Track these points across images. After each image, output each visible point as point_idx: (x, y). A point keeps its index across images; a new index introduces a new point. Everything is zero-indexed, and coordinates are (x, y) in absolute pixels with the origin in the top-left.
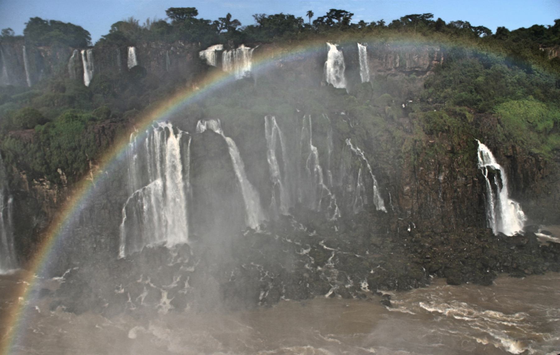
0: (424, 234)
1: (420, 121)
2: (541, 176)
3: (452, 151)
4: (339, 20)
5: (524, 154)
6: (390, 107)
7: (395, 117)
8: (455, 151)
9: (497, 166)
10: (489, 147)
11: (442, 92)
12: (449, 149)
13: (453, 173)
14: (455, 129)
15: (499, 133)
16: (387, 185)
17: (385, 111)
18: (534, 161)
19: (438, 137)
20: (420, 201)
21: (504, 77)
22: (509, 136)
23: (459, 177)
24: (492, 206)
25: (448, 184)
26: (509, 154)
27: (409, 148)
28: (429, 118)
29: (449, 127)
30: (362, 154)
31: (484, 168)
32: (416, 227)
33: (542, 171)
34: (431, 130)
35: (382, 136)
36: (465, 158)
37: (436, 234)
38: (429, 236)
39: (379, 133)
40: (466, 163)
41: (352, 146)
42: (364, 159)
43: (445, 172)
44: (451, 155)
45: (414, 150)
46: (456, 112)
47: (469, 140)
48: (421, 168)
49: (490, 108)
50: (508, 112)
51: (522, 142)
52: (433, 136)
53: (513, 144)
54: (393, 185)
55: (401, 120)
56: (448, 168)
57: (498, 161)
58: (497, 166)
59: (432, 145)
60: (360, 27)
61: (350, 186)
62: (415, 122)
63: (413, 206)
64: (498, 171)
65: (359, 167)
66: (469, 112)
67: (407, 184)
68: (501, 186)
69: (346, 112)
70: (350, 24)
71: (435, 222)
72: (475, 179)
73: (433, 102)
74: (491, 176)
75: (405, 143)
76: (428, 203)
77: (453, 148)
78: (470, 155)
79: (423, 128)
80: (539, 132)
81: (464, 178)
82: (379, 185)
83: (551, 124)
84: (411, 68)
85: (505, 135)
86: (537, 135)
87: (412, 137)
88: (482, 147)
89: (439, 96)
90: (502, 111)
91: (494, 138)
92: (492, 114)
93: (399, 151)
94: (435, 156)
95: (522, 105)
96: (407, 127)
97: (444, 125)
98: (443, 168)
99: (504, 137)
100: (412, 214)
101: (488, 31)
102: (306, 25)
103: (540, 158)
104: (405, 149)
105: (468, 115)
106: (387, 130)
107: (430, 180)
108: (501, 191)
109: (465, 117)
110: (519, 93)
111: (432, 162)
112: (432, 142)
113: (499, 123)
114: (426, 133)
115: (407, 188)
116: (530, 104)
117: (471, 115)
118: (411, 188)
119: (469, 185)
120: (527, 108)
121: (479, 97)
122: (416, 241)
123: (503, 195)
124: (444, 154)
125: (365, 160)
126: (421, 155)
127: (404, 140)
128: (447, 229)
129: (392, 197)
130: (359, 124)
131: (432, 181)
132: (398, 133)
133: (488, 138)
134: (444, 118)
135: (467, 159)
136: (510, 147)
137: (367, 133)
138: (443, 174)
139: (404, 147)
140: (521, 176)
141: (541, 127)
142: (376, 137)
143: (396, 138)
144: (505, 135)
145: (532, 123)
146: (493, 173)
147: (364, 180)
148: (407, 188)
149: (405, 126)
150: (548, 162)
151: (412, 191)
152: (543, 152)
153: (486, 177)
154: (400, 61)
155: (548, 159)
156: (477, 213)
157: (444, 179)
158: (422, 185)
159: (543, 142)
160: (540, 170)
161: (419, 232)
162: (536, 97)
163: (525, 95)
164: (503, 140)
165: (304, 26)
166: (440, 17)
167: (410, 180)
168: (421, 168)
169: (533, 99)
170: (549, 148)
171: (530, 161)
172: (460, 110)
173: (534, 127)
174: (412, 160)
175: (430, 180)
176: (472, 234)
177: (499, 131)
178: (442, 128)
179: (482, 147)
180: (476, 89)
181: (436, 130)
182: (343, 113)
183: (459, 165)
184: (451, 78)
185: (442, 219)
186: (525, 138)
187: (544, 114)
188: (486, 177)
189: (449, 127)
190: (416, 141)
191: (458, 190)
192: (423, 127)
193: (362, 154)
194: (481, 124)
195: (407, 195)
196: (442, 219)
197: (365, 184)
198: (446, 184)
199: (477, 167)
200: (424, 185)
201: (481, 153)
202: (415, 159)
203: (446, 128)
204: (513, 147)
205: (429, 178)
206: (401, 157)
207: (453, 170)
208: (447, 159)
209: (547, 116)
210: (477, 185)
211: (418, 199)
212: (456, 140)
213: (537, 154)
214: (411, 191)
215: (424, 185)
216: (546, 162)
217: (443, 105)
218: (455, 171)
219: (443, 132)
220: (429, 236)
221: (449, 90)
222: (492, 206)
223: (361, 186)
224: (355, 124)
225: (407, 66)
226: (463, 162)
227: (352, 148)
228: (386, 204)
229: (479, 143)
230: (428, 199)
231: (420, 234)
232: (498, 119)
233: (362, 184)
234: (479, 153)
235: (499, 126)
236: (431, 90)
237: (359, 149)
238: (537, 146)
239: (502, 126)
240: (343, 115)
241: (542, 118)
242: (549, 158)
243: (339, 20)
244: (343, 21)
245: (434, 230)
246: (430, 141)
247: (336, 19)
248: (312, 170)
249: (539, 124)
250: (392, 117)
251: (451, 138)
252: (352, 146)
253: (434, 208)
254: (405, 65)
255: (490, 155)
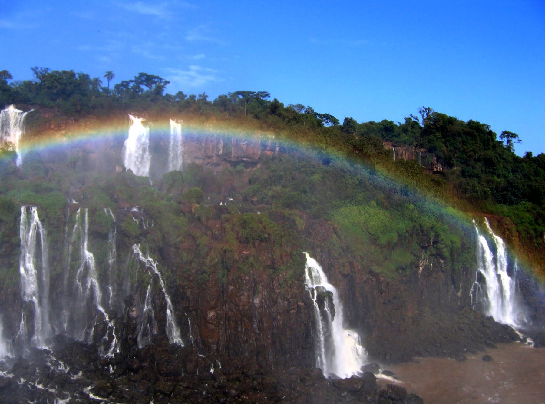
0: (231, 378)
1: (234, 225)
6: (198, 205)
7: (203, 219)
8: (276, 266)
9: (329, 287)
10: (321, 262)
12: (269, 263)
13: (273, 295)
15: (334, 245)
16: (186, 309)
23: (280, 300)
25: (265, 309)
26: (346, 273)
27: (217, 260)
30: (155, 265)
31: (313, 290)
32: (222, 366)
35: (182, 242)
36: (288, 276)
37: (247, 376)
38: (238, 379)
40: (290, 283)
41: (141, 254)
42: (157, 272)
44: (271, 271)
45: (223, 262)
47: (294, 253)
48: (232, 288)
50: (346, 220)
51: (362, 258)
54: (193, 310)
58: (329, 287)
59: (247, 257)
61: (134, 309)
63: (219, 339)
64: (329, 294)
65: (148, 284)
67: (213, 308)
69: (139, 209)
72: (300, 304)
74: (320, 301)
77: (273, 263)
79: (238, 235)
81: (286, 303)
82: (175, 309)
85: (342, 248)
92: (327, 221)
94: (249, 272)
96: (217, 233)
98: (261, 288)
100: (218, 349)
104: (211, 261)
107: (241, 304)
111: (246, 280)
113: (336, 233)
114: (240, 242)
115: (212, 314)
118: (217, 313)
119: (292, 312)
122: (219, 387)
124: (261, 269)
125: (157, 275)
129: (192, 325)
130: (155, 225)
131: (243, 305)
135: (291, 277)
136: (347, 264)
137: (164, 238)
138: (260, 295)
139: (209, 258)
143: (201, 246)
144: (342, 248)
146: (324, 296)
147: (153, 302)
148: (212, 314)
149: (214, 231)
151: (217, 317)
153: (314, 300)
157: (261, 302)
158: (232, 311)
161: (225, 374)
164: (340, 254)
166: (276, 98)
168: (232, 288)
174: (220, 275)
175: (241, 304)
182: (135, 209)
183: (280, 285)
191: (279, 317)
193: (155, 265)
195: (212, 323)
197: (154, 308)
198: (263, 310)
199: (303, 288)
200: (234, 310)
202: (223, 276)
204: (351, 264)
206: (205, 272)
208: (265, 276)
210: (302, 311)
211: (226, 329)
214: (217, 318)
215: (234, 310)
220: (238, 379)
223: (149, 311)
227: (141, 257)
228: (184, 335)
229: (307, 256)
230: (239, 329)
231: (225, 377)
232: (334, 228)
233: (150, 307)
235: (334, 236)
237: (151, 260)
239: (339, 237)
240: (135, 212)
245: (245, 370)
248: (84, 283)
251: (272, 250)
252: (141, 254)
255: (322, 274)
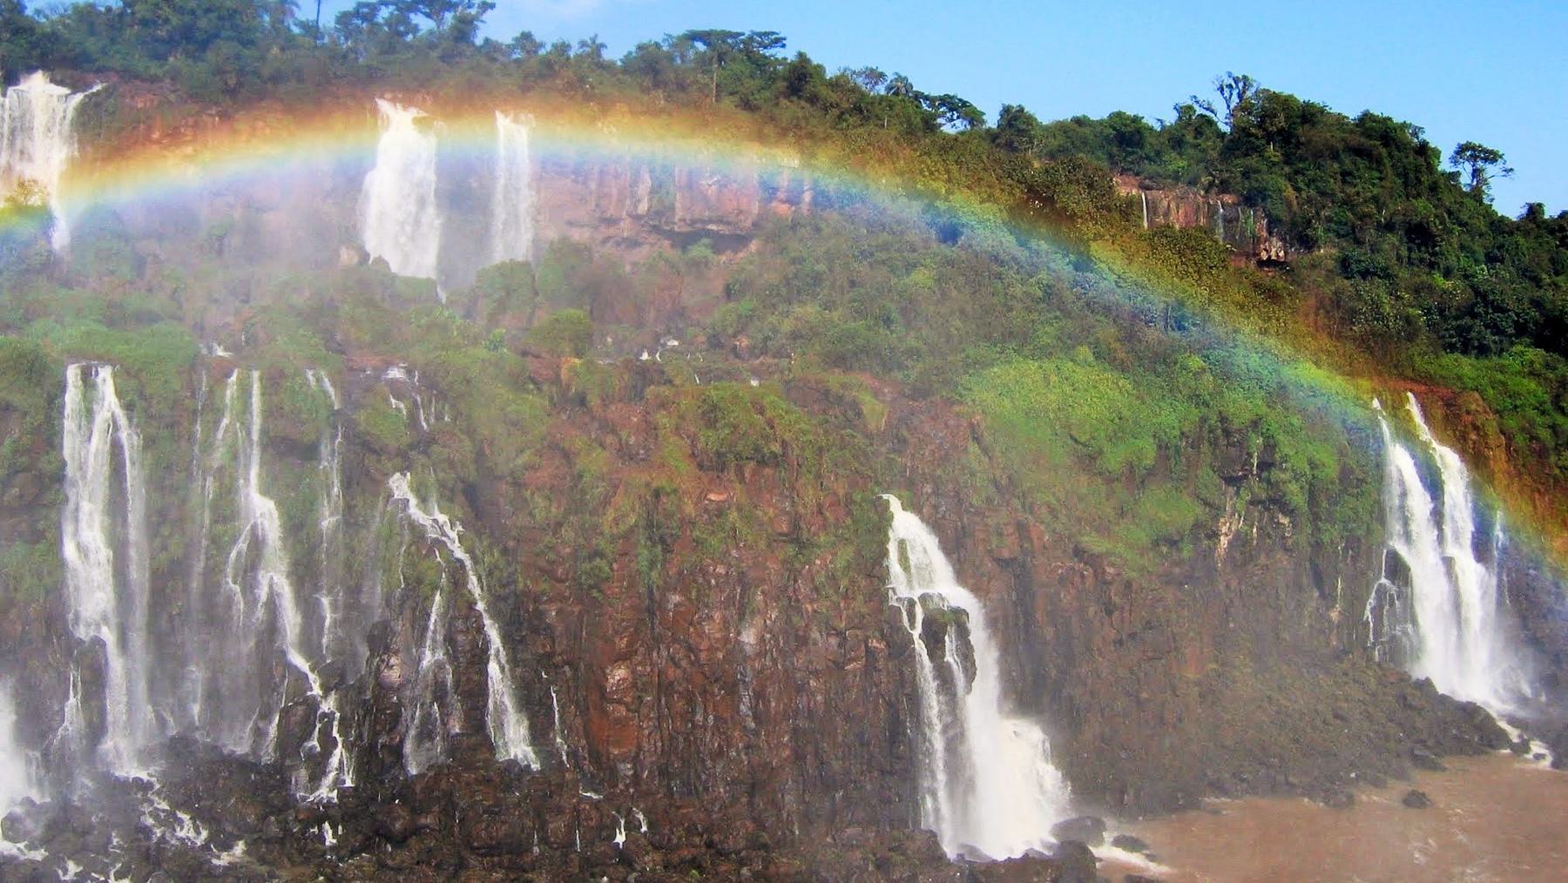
2: (1113, 635)
3: (795, 537)
4: (440, 22)
5: (1059, 553)
8: (805, 536)
9: (957, 596)
10: (935, 524)
11: (787, 314)
12: (785, 528)
13: (795, 619)
14: (808, 453)
15: (973, 475)
17: (558, 376)
18: (1090, 582)
19: (742, 480)
20: (668, 725)
21: (999, 277)
22: (1007, 488)
23: (815, 635)
24: (939, 744)
25: (774, 661)
26: (1006, 554)
27: (632, 520)
28: (714, 407)
29: (784, 444)
33: (1116, 614)
34: (719, 455)
36: (840, 563)
39: (526, 457)
40: (843, 584)
43: (763, 614)
44: (791, 550)
46: (827, 392)
47: (858, 497)
48: (676, 598)
49: (945, 383)
50: (1007, 402)
52: (725, 476)
53: (1021, 516)
55: (615, 411)
56: (777, 599)
57: (962, 575)
58: (957, 596)
59: (720, 512)
60: (518, 55)
62: (663, 419)
64: (959, 616)
66: (876, 394)
67: (623, 657)
68: (970, 672)
70: (479, 41)
71: (723, 807)
72: (875, 644)
73: (753, 351)
75: (619, 499)
76: (699, 733)
78: (858, 553)
79: (693, 445)
80: (1110, 480)
81: (833, 641)
83: (1150, 455)
84: (693, 222)
85: (995, 483)
86: (1103, 488)
87: (645, 478)
88: (906, 525)
89: (775, 331)
90: (988, 397)
91: (957, 493)
92: (953, 404)
93: (596, 530)
94: (728, 552)
95: (1054, 378)
97: (766, 437)
98: (760, 598)
99: (992, 490)
101: (973, 116)
102: (304, 25)
103: (1111, 570)
104: (616, 521)
105: (869, 403)
106: (554, 447)
107: (704, 645)
108: (969, 689)
109: (859, 414)
110: (1047, 334)
111: (717, 576)
112: (722, 498)
113: (977, 440)
114: (700, 466)
115: (619, 674)
116: (1080, 375)
117: (879, 407)
118: (633, 672)
120: (1068, 390)
121: (912, 341)
123: (982, 699)
124: (762, 545)
126: (676, 548)
127: (616, 487)
128: (765, 837)
130: (455, 419)
131: (711, 649)
132: (595, 462)
133: (936, 493)
134: (769, 414)
135: (848, 567)
137: (480, 456)
138: (758, 621)
139: (611, 514)
140: (1049, 633)
141: (1114, 459)
142: (512, 473)
143: (587, 478)
144: (995, 483)
145: (1084, 445)
146: (941, 625)
150: (1135, 585)
152: (1120, 548)
154: (653, 192)
155: (1134, 575)
156: (882, 772)
157: (762, 640)
158: (677, 665)
159: (1122, 514)
160: (1109, 613)
162: (1102, 355)
163: (1067, 343)
164: (989, 500)
165: (296, 30)
167: (630, 644)
168: (676, 598)
169: (1091, 358)
170: (1143, 536)
171: (1077, 579)
172: (844, 386)
173: (1092, 458)
174: (643, 563)
175: (704, 645)
176: (858, 854)
177: (975, 465)
178: (757, 449)
179: (906, 525)
180: (904, 311)
181: (738, 457)
183: (816, 589)
184: (821, 267)
185: (751, 795)
186: (1062, 496)
187: (1125, 413)
188: (916, 633)
189: (784, 444)
190: (657, 494)
192: (694, 440)
194: (913, 441)
196: (751, 795)
199: (885, 598)
200: (684, 663)
201: (902, 544)
202: (652, 564)
203: (776, 448)
205: (701, 635)
207: (792, 606)
209: (1136, 423)
210: (881, 664)
212: (810, 496)
213: (1100, 556)
214: (634, 685)
215: (684, 663)
216: (1128, 585)
217: (784, 362)
218: (799, 611)
219: (762, 463)
221: (809, 311)
222: (939, 744)
224: (439, 417)
225: (679, 214)
226: (833, 579)
229: (895, 504)
230: (699, 717)
232: (971, 425)
234: (892, 548)
235: (973, 448)
236: (745, 305)
238: (1103, 530)
239: (985, 451)
241: (1121, 429)
242: (1143, 569)
243: (440, 22)
244: (453, 28)
246: (712, 497)
247: (428, 16)
249: (1107, 448)
250: (582, 401)
253: (720, 753)
254: (672, 208)
